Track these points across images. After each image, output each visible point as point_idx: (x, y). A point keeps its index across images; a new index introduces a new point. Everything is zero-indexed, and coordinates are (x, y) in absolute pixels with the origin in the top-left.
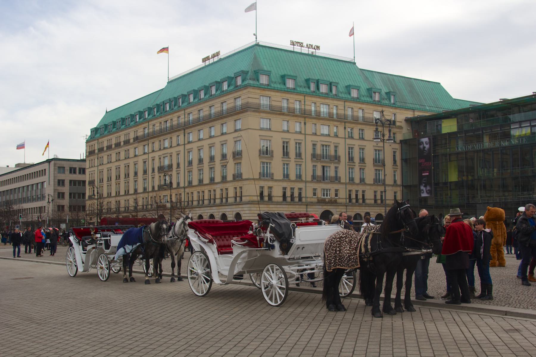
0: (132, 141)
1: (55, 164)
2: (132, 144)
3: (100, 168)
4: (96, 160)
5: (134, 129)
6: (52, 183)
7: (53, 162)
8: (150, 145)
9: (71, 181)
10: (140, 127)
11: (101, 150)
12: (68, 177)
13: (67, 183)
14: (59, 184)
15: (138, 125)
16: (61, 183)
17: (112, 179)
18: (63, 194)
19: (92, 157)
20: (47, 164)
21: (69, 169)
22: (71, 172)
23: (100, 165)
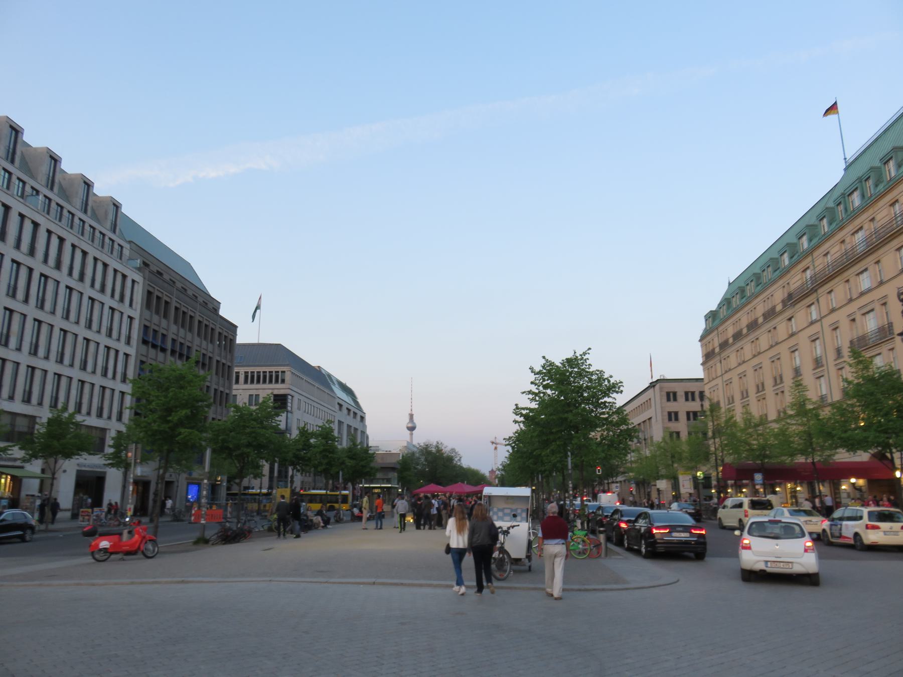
0: (779, 308)
1: (661, 389)
2: (781, 312)
3: (726, 377)
4: (718, 365)
5: (781, 282)
6: (659, 418)
7: (657, 387)
8: (822, 300)
9: (688, 413)
10: (792, 272)
11: (724, 345)
12: (682, 406)
13: (683, 417)
14: (670, 419)
15: (788, 271)
16: (673, 416)
17: (750, 394)
18: (678, 433)
19: (711, 363)
20: (651, 391)
21: (683, 394)
22: (687, 399)
23: (726, 372)
